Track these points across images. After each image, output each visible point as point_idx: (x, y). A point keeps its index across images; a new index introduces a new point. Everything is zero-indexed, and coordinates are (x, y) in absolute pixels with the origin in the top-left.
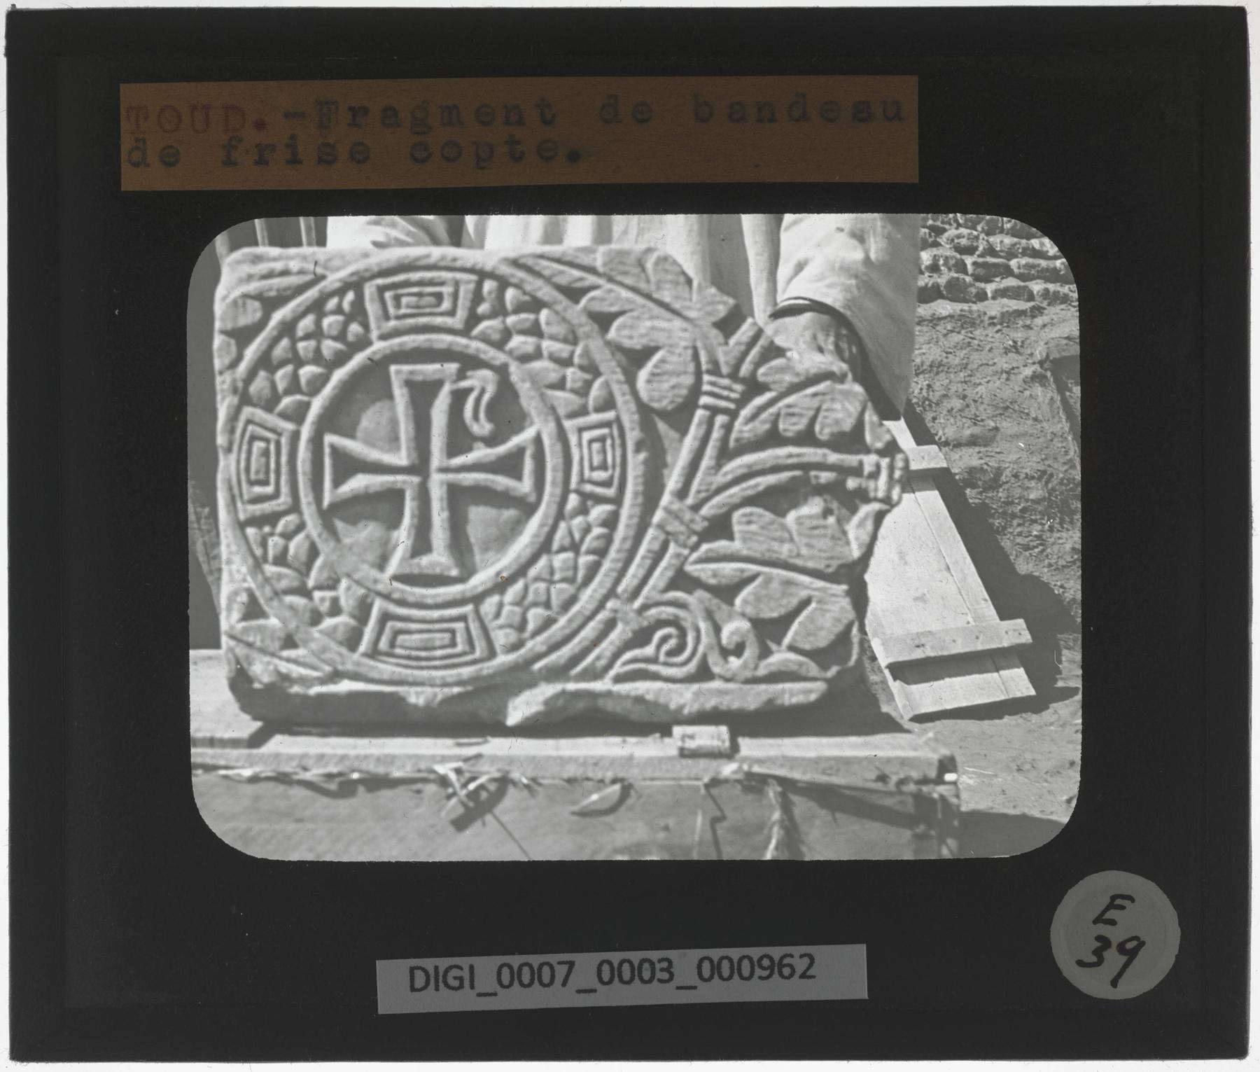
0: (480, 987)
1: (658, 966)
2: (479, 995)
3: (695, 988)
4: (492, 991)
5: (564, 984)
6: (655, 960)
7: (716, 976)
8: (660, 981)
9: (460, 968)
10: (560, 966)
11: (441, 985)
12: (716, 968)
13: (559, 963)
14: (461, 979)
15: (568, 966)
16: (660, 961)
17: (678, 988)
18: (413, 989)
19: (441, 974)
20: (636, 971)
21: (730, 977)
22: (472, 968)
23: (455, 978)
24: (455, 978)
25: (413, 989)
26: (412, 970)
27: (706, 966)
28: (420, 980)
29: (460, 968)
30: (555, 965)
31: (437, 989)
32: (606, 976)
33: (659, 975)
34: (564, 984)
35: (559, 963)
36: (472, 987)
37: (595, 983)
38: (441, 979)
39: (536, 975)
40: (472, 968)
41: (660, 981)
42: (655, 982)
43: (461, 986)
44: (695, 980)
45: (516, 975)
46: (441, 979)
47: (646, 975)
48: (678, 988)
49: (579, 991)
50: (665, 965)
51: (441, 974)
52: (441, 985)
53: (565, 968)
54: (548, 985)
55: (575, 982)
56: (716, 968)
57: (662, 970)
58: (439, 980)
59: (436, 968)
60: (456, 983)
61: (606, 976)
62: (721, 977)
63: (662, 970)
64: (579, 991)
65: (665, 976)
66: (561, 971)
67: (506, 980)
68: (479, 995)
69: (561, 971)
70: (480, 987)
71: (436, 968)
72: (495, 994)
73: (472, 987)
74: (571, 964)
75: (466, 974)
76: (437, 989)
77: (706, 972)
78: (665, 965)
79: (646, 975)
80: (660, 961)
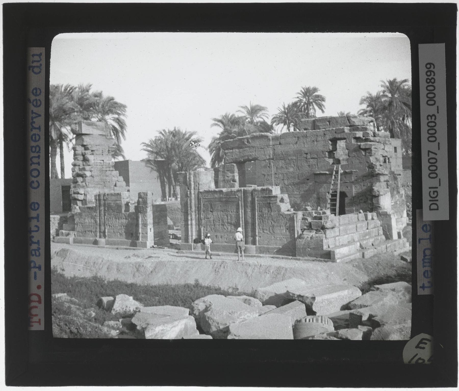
0: (438, 186)
1: (430, 120)
2: (440, 185)
3: (438, 107)
4: (439, 180)
5: (436, 154)
6: (427, 121)
7: (434, 99)
8: (435, 119)
9: (430, 192)
10: (430, 155)
11: (436, 199)
12: (431, 99)
13: (428, 156)
14: (434, 192)
15: (430, 153)
16: (428, 119)
17: (438, 112)
18: (437, 209)
19: (431, 199)
20: (432, 128)
21: (434, 94)
22: (430, 188)
23: (434, 194)
24: (434, 194)
25: (437, 209)
26: (430, 209)
27: (430, 102)
28: (434, 207)
29: (430, 192)
30: (429, 158)
31: (437, 200)
32: (433, 139)
33: (433, 120)
34: (436, 154)
35: (428, 156)
36: (437, 188)
37: (436, 143)
38: (434, 199)
39: (433, 164)
40: (430, 188)
41: (435, 119)
42: (436, 121)
43: (437, 192)
44: (435, 107)
45: (433, 172)
46: (434, 199)
47: (433, 124)
48: (438, 112)
49: (439, 149)
50: (429, 118)
51: (431, 199)
52: (436, 199)
53: (430, 153)
54: (436, 159)
55: (436, 151)
56: (431, 99)
57: (431, 119)
58: (434, 200)
59: (430, 201)
60: (436, 193)
61: (433, 139)
62: (434, 97)
63: (431, 119)
64: (439, 149)
65: (433, 117)
66: (432, 155)
67: (434, 175)
68: (440, 185)
69: (432, 155)
70: (438, 186)
71: (430, 201)
72: (440, 179)
73: (437, 188)
74: (429, 151)
75: (432, 190)
76: (437, 200)
77: (432, 102)
78: (429, 118)
79: (433, 124)
80: (428, 119)
